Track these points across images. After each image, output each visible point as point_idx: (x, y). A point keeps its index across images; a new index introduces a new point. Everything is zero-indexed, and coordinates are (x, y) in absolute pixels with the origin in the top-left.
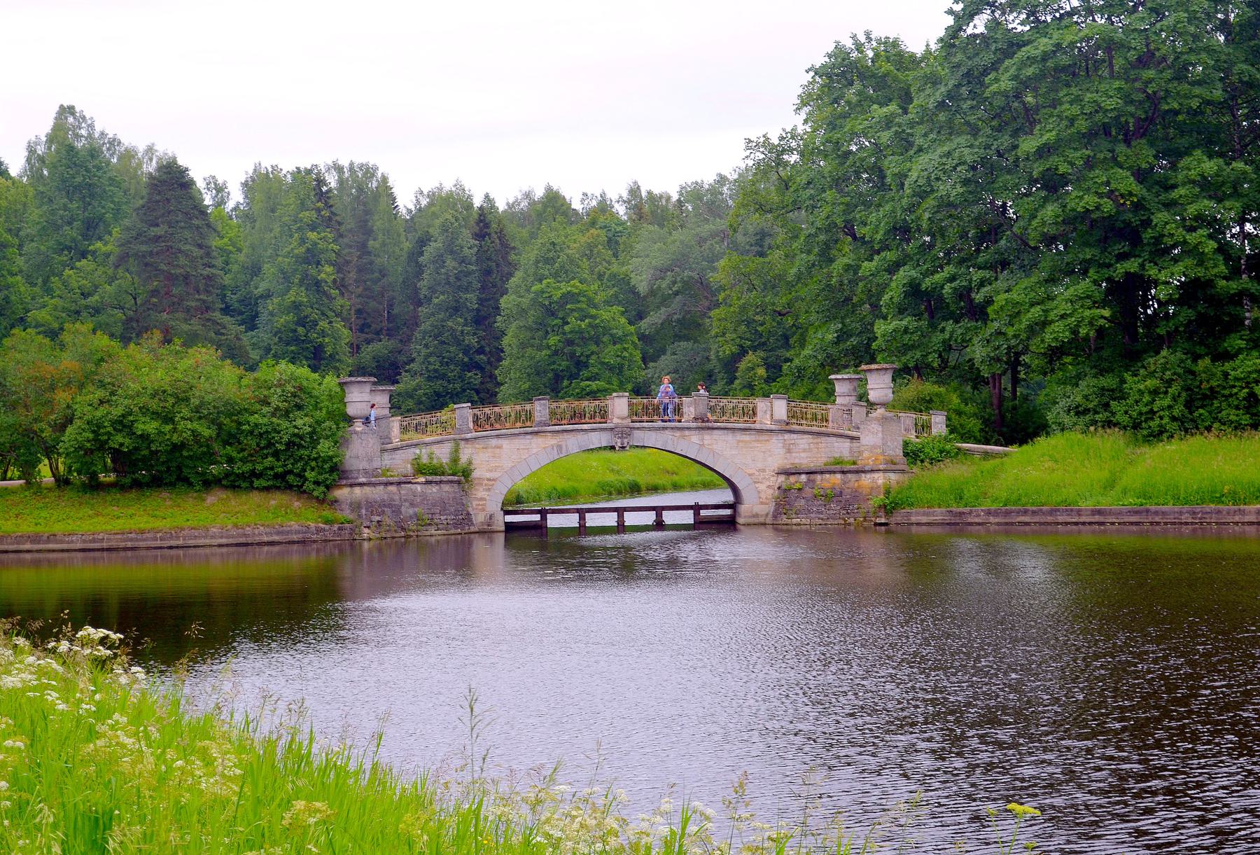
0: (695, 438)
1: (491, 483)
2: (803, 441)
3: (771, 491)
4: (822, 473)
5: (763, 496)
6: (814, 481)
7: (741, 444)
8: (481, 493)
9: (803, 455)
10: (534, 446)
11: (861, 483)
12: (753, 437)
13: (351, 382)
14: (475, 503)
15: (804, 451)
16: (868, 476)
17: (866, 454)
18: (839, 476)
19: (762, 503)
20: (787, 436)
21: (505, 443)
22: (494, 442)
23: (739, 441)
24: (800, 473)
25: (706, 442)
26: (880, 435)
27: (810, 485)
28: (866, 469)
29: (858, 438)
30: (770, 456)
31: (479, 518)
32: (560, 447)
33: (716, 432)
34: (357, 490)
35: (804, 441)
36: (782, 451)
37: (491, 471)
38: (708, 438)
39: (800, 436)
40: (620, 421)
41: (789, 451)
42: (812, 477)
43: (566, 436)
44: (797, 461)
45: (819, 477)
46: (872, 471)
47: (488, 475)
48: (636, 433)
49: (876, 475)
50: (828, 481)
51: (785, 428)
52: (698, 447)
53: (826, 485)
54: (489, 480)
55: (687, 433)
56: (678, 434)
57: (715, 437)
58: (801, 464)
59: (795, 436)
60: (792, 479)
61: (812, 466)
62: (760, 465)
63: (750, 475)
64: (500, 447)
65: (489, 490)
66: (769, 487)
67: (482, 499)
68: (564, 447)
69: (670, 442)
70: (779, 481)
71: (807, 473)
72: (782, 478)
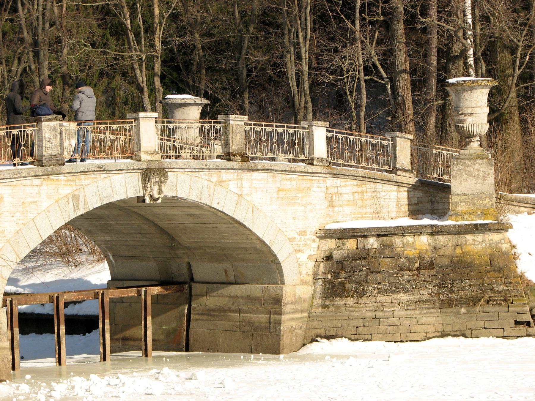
6: (391, 247)
7: (282, 194)
11: (467, 249)
15: (348, 203)
16: (479, 238)
19: (304, 283)
25: (245, 191)
27: (387, 252)
40: (149, 158)
41: (332, 204)
45: (398, 241)
50: (413, 245)
53: (411, 253)
56: (215, 178)
59: (338, 182)
60: (351, 244)
63: (291, 240)
66: (310, 257)
68: (82, 199)
69: (206, 190)
71: (379, 236)
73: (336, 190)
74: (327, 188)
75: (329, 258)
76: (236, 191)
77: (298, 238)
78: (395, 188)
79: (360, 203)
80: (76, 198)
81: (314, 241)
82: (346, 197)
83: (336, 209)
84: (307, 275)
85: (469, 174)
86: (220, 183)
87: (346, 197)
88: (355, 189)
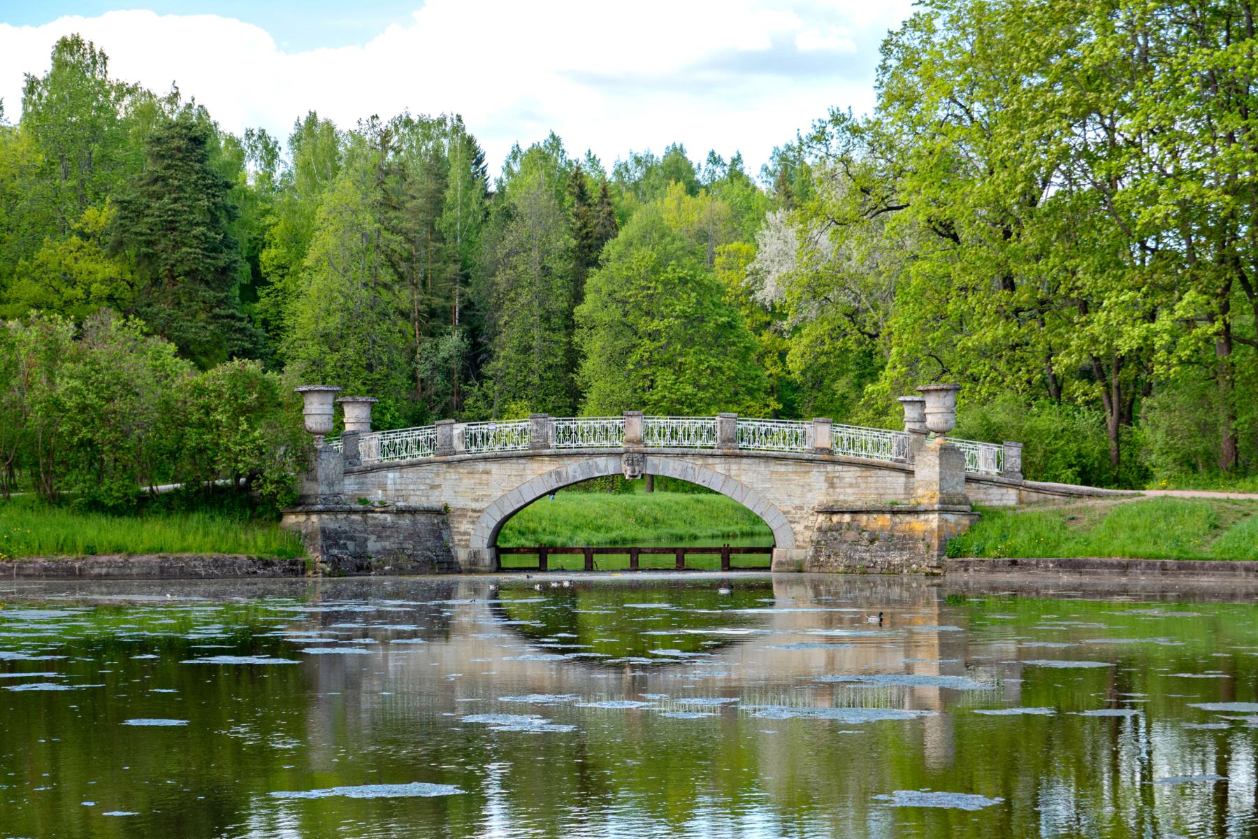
0: (719, 467)
1: (476, 515)
2: (850, 474)
3: (808, 533)
4: (868, 512)
5: (800, 538)
8: (464, 526)
9: (849, 491)
10: (529, 472)
12: (790, 468)
13: (310, 391)
14: (456, 538)
15: (851, 485)
16: (922, 517)
17: (920, 492)
18: (888, 516)
19: (798, 547)
20: (830, 468)
21: (494, 468)
22: (481, 466)
23: (773, 472)
24: (843, 512)
25: (733, 473)
26: (937, 469)
28: (921, 508)
29: (910, 473)
30: (810, 491)
31: (462, 555)
32: (558, 474)
33: (745, 460)
34: (314, 518)
35: (850, 474)
36: (826, 485)
37: (477, 500)
38: (735, 467)
39: (846, 468)
41: (832, 485)
42: (859, 517)
43: (566, 461)
44: (841, 497)
45: (864, 517)
46: (926, 512)
47: (474, 505)
48: (649, 458)
49: (931, 516)
51: (827, 457)
52: (723, 477)
54: (474, 511)
55: (710, 461)
56: (700, 462)
57: (743, 467)
58: (846, 502)
59: (839, 468)
60: (835, 518)
61: (859, 505)
62: (797, 502)
63: (785, 513)
64: (487, 473)
65: (473, 522)
66: (806, 527)
67: (465, 533)
69: (690, 471)
70: (819, 521)
72: (821, 518)
73: (837, 475)
74: (828, 472)
75: (819, 529)
76: (723, 472)
77: (794, 511)
78: (903, 475)
79: (863, 486)
80: (558, 474)
81: (812, 515)
82: (847, 480)
83: (838, 490)
84: (804, 541)
85: (925, 463)
86: (706, 465)
87: (847, 480)
88: (858, 474)
